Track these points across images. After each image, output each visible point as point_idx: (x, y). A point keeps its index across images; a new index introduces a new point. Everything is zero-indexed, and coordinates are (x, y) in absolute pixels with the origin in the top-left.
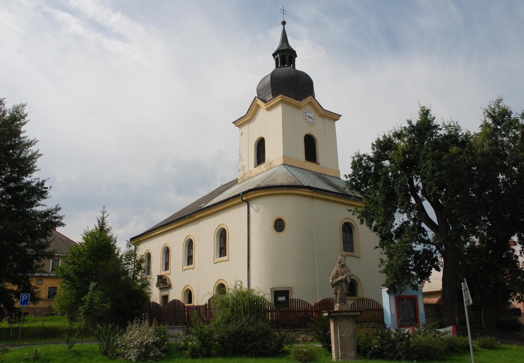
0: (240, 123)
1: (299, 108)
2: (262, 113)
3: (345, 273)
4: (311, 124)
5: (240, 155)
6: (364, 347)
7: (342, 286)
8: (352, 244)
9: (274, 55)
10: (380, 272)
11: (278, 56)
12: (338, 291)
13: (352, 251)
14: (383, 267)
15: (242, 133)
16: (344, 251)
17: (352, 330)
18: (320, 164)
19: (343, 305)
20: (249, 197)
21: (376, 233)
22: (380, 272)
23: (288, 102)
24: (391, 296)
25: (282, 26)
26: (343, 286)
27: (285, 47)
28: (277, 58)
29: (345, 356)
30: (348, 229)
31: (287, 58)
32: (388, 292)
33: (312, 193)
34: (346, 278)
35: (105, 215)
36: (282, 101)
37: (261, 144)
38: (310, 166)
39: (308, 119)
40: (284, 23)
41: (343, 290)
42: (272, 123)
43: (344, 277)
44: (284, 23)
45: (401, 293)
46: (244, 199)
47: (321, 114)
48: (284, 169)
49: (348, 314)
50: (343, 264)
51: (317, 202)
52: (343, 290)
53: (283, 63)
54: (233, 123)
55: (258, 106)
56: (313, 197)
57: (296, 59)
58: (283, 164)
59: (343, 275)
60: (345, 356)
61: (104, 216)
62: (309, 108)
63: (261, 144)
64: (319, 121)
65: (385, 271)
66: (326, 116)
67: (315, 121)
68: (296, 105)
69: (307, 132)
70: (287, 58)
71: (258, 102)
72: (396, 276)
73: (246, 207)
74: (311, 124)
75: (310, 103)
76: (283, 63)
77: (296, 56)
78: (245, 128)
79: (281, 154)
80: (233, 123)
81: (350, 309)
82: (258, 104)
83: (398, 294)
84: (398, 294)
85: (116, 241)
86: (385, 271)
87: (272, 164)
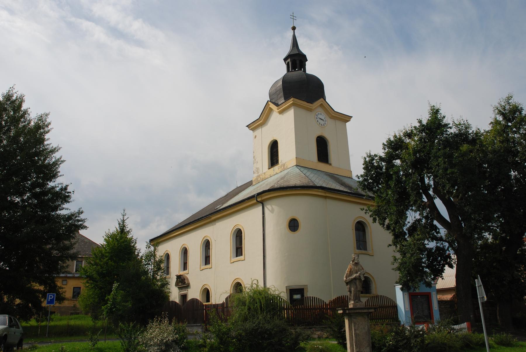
0: (254, 126)
1: (310, 110)
2: (275, 116)
3: (359, 271)
6: (379, 344)
7: (355, 283)
8: (365, 242)
9: (285, 60)
10: (393, 269)
11: (289, 60)
13: (365, 249)
14: (396, 265)
15: (256, 137)
16: (358, 249)
17: (366, 328)
18: (333, 165)
20: (263, 198)
21: (389, 231)
22: (393, 269)
24: (405, 293)
25: (292, 31)
26: (357, 283)
28: (288, 63)
30: (360, 227)
31: (298, 62)
32: (402, 289)
33: (325, 193)
35: (125, 218)
36: (293, 104)
37: (274, 147)
38: (323, 167)
39: (320, 121)
40: (294, 28)
41: (357, 288)
42: (284, 126)
44: (294, 28)
45: (414, 290)
46: (259, 200)
48: (297, 170)
49: (363, 311)
51: (329, 201)
52: (357, 288)
53: (294, 67)
55: (271, 110)
56: (326, 197)
57: (307, 63)
58: (296, 165)
59: (357, 273)
62: (320, 110)
63: (274, 147)
64: (330, 122)
65: (399, 269)
70: (298, 62)
71: (270, 106)
72: (409, 273)
73: (260, 208)
76: (294, 67)
78: (258, 132)
79: (294, 156)
81: (364, 306)
83: (411, 291)
84: (411, 291)
85: (136, 243)
86: (399, 269)
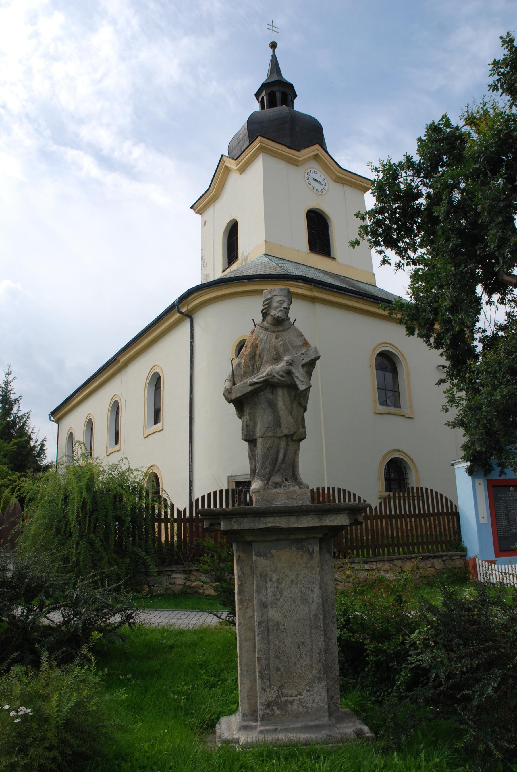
0: (200, 206)
1: (295, 163)
2: (235, 180)
3: (286, 351)
4: (320, 193)
5: (202, 259)
6: (377, 652)
7: (273, 406)
8: (396, 392)
9: (257, 95)
10: (448, 424)
11: (263, 94)
12: (260, 429)
13: (397, 404)
14: (454, 412)
15: (205, 222)
16: (381, 403)
17: (315, 596)
18: (338, 260)
19: (277, 485)
20: (190, 306)
21: (441, 351)
22: (448, 424)
23: (274, 152)
24: (477, 481)
25: (271, 51)
26: (280, 404)
27: (275, 78)
28: (263, 98)
29: (283, 706)
30: (387, 363)
31: (278, 95)
32: (470, 471)
33: (311, 290)
34: (289, 373)
35: (11, 378)
36: (262, 149)
37: (232, 233)
38: (319, 261)
39: (314, 183)
40: (274, 45)
41: (277, 423)
42: (249, 196)
43: (281, 366)
44: (274, 45)
45: (502, 472)
46: (183, 310)
47: (338, 177)
48: (266, 259)
49: (293, 523)
50: (279, 314)
51: (321, 310)
52: (277, 423)
53: (272, 104)
54: (191, 208)
55: (228, 170)
56: (313, 300)
57: (296, 101)
58: (266, 255)
59: (277, 359)
60: (283, 706)
61: (10, 380)
62: (314, 166)
63: (232, 233)
64: (335, 190)
65: (460, 423)
66: (347, 180)
67: (326, 188)
68: (290, 158)
69: (312, 204)
70: (278, 95)
71: (226, 164)
72: (489, 433)
73: (186, 326)
74: (320, 193)
75: (316, 157)
76: (272, 104)
77: (295, 96)
78: (210, 211)
79: (262, 238)
80: (191, 208)
81: (308, 502)
82: (227, 167)
83: (495, 475)
84: (495, 475)
85: (28, 417)
86: (460, 423)
87: (249, 259)
